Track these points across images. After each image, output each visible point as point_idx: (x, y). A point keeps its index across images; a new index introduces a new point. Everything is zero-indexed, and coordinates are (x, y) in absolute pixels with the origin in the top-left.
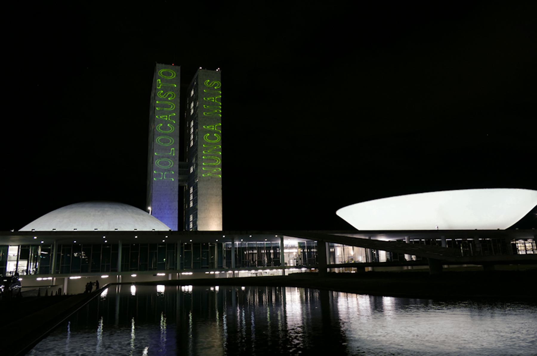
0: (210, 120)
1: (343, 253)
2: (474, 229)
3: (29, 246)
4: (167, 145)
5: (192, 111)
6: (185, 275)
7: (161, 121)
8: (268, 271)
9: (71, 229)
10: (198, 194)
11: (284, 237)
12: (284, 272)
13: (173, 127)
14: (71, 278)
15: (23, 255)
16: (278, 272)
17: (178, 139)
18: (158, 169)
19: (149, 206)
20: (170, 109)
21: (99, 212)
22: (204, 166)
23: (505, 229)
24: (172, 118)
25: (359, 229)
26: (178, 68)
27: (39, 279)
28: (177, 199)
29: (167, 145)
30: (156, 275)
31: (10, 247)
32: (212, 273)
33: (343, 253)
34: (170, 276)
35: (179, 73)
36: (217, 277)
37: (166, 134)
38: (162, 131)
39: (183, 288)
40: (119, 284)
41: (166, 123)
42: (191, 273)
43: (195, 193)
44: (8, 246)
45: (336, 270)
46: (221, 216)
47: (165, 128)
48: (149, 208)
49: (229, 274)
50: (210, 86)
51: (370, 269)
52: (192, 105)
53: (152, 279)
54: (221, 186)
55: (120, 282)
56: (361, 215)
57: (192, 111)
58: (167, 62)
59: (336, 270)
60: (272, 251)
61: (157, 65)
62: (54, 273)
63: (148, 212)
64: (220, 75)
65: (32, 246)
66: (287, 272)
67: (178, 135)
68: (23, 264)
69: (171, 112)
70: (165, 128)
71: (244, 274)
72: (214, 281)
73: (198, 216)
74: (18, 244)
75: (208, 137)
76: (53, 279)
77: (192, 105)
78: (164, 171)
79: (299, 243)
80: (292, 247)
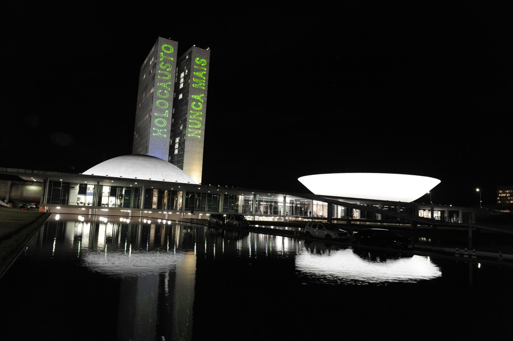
0: (198, 91)
2: (398, 201)
3: (116, 187)
4: (163, 107)
9: (173, 180)
10: (185, 150)
15: (113, 193)
16: (276, 219)
17: (172, 103)
22: (191, 128)
23: (409, 201)
24: (168, 86)
25: (316, 192)
29: (163, 107)
35: (177, 48)
38: (160, 96)
41: (163, 89)
44: (102, 186)
45: (335, 222)
47: (162, 93)
50: (201, 62)
51: (335, 222)
54: (203, 146)
61: (160, 38)
64: (209, 54)
65: (119, 187)
68: (113, 199)
69: (167, 81)
70: (162, 93)
75: (195, 105)
78: (160, 128)
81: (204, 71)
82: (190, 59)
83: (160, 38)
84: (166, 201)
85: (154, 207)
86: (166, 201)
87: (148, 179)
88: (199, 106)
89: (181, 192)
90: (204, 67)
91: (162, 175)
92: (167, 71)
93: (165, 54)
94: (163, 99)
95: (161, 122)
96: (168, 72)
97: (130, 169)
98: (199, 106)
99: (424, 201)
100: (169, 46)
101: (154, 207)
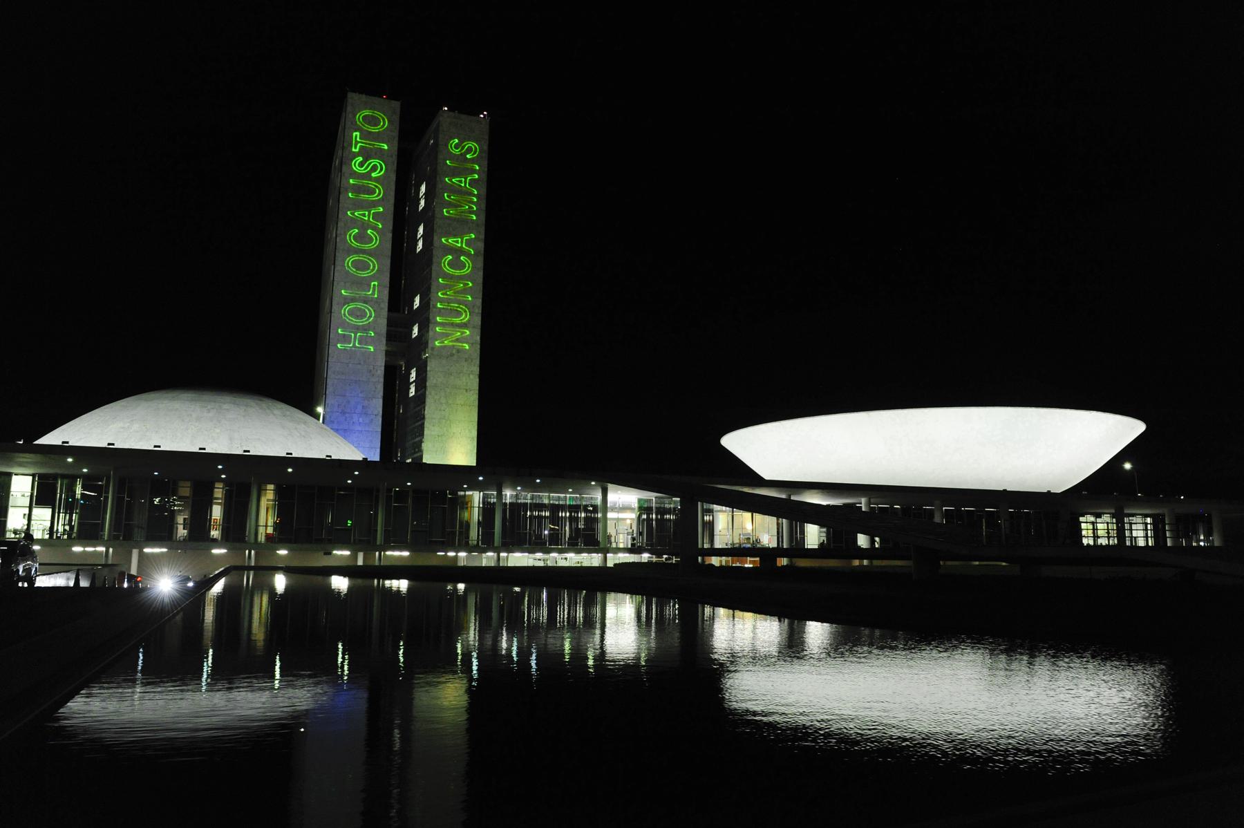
1: (731, 526)
3: (55, 477)
4: (364, 274)
5: (422, 202)
7: (354, 222)
8: (571, 555)
11: (610, 486)
12: (605, 559)
13: (377, 239)
14: (146, 550)
15: (43, 495)
16: (592, 560)
17: (388, 262)
18: (344, 325)
19: (318, 404)
20: (374, 197)
21: (209, 411)
24: (376, 216)
25: (767, 476)
26: (396, 105)
27: (77, 549)
28: (381, 394)
29: (364, 274)
30: (330, 554)
31: (14, 477)
32: (451, 554)
33: (731, 526)
35: (397, 118)
36: (461, 563)
37: (364, 252)
38: (355, 244)
39: (388, 583)
40: (249, 568)
41: (364, 226)
42: (406, 554)
43: (421, 383)
44: (9, 475)
45: (715, 561)
46: (475, 433)
47: (362, 237)
48: (320, 410)
49: (488, 559)
50: (464, 151)
51: (784, 561)
52: (423, 188)
54: (476, 370)
56: (775, 448)
57: (422, 202)
58: (373, 88)
59: (715, 561)
62: (109, 539)
63: (317, 416)
65: (63, 477)
66: (612, 560)
67: (390, 254)
68: (43, 515)
69: (374, 204)
70: (362, 237)
71: (518, 559)
72: (456, 573)
74: (31, 472)
76: (107, 551)
77: (423, 188)
78: (357, 329)
79: (640, 500)
80: (624, 509)
81: (474, 171)
82: (436, 144)
84: (217, 512)
85: (182, 532)
86: (217, 512)
87: (104, 445)
88: (462, 266)
89: (271, 487)
90: (472, 161)
91: (231, 439)
92: (371, 179)
93: (365, 135)
94: (364, 252)
95: (359, 314)
96: (376, 180)
97: (136, 426)
98: (462, 266)
99: (1104, 487)
100: (378, 114)
101: (182, 532)
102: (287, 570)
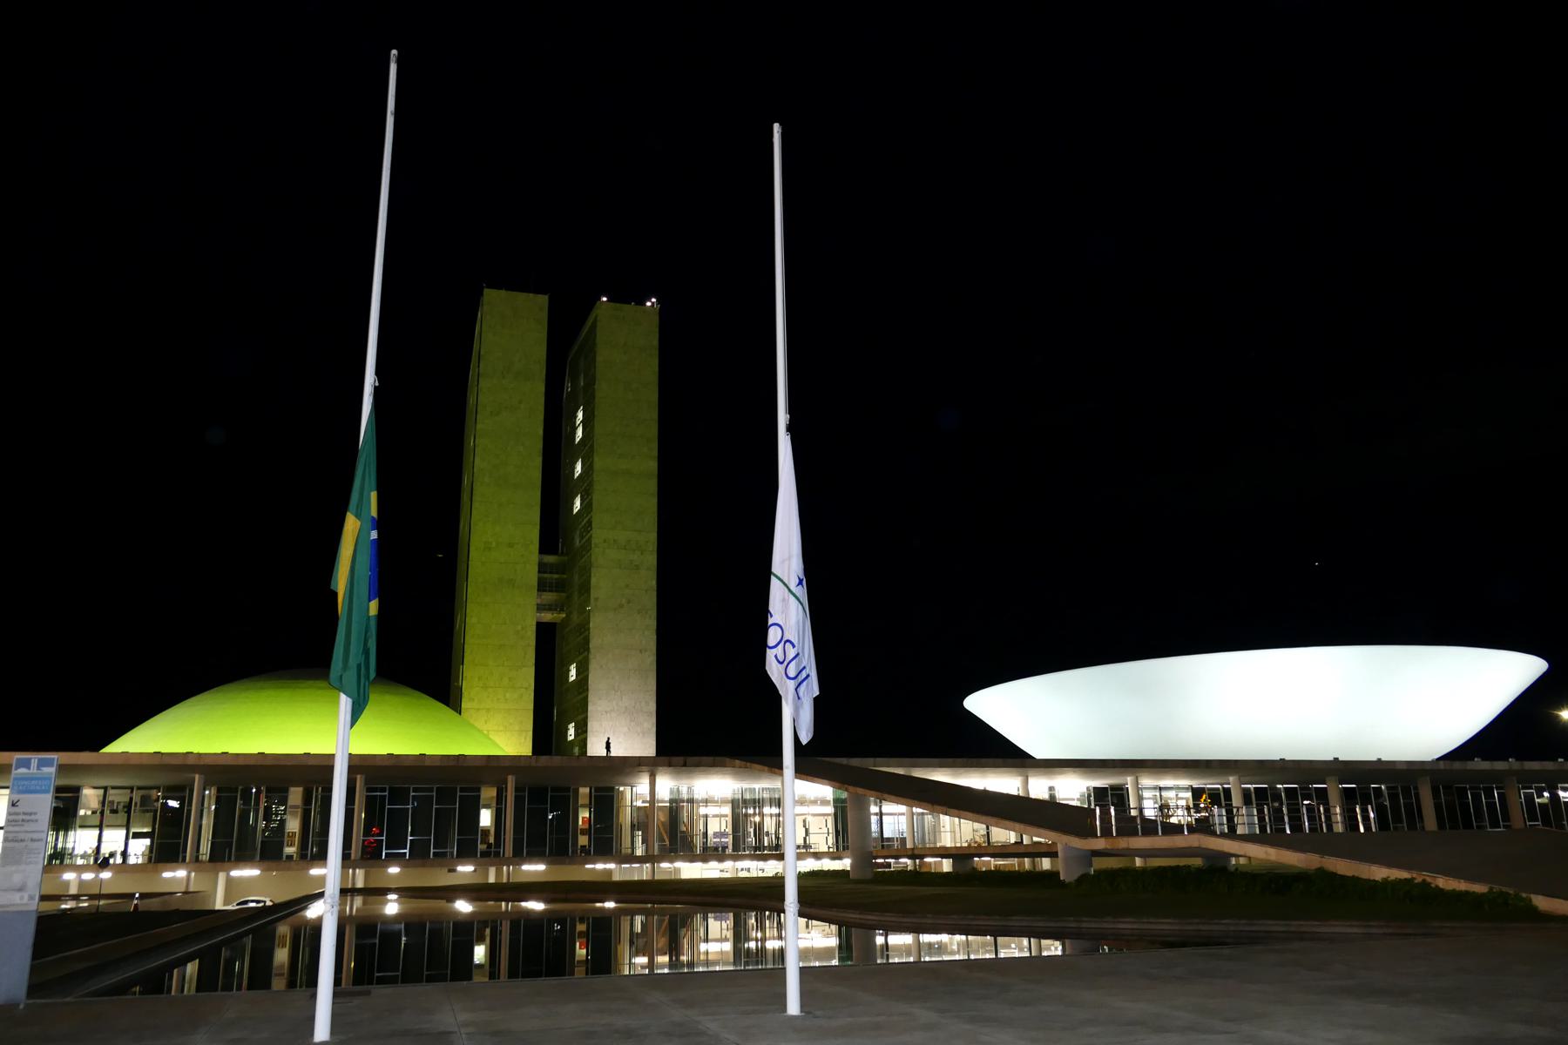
6: (529, 872)
8: (728, 864)
14: (235, 873)
26: (543, 300)
32: (600, 866)
34: (492, 872)
39: (524, 904)
42: (541, 867)
46: (653, 707)
53: (441, 878)
54: (653, 623)
55: (360, 884)
60: (751, 811)
61: (486, 291)
73: (590, 708)
80: (824, 802)
83: (486, 291)
102: (405, 892)
